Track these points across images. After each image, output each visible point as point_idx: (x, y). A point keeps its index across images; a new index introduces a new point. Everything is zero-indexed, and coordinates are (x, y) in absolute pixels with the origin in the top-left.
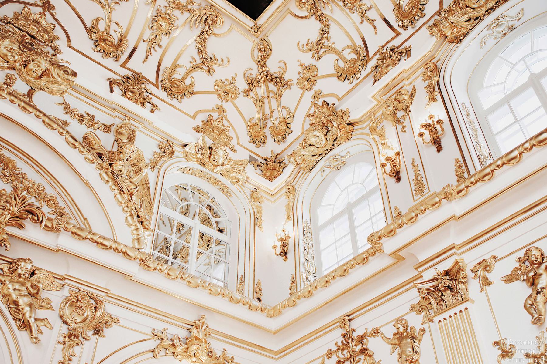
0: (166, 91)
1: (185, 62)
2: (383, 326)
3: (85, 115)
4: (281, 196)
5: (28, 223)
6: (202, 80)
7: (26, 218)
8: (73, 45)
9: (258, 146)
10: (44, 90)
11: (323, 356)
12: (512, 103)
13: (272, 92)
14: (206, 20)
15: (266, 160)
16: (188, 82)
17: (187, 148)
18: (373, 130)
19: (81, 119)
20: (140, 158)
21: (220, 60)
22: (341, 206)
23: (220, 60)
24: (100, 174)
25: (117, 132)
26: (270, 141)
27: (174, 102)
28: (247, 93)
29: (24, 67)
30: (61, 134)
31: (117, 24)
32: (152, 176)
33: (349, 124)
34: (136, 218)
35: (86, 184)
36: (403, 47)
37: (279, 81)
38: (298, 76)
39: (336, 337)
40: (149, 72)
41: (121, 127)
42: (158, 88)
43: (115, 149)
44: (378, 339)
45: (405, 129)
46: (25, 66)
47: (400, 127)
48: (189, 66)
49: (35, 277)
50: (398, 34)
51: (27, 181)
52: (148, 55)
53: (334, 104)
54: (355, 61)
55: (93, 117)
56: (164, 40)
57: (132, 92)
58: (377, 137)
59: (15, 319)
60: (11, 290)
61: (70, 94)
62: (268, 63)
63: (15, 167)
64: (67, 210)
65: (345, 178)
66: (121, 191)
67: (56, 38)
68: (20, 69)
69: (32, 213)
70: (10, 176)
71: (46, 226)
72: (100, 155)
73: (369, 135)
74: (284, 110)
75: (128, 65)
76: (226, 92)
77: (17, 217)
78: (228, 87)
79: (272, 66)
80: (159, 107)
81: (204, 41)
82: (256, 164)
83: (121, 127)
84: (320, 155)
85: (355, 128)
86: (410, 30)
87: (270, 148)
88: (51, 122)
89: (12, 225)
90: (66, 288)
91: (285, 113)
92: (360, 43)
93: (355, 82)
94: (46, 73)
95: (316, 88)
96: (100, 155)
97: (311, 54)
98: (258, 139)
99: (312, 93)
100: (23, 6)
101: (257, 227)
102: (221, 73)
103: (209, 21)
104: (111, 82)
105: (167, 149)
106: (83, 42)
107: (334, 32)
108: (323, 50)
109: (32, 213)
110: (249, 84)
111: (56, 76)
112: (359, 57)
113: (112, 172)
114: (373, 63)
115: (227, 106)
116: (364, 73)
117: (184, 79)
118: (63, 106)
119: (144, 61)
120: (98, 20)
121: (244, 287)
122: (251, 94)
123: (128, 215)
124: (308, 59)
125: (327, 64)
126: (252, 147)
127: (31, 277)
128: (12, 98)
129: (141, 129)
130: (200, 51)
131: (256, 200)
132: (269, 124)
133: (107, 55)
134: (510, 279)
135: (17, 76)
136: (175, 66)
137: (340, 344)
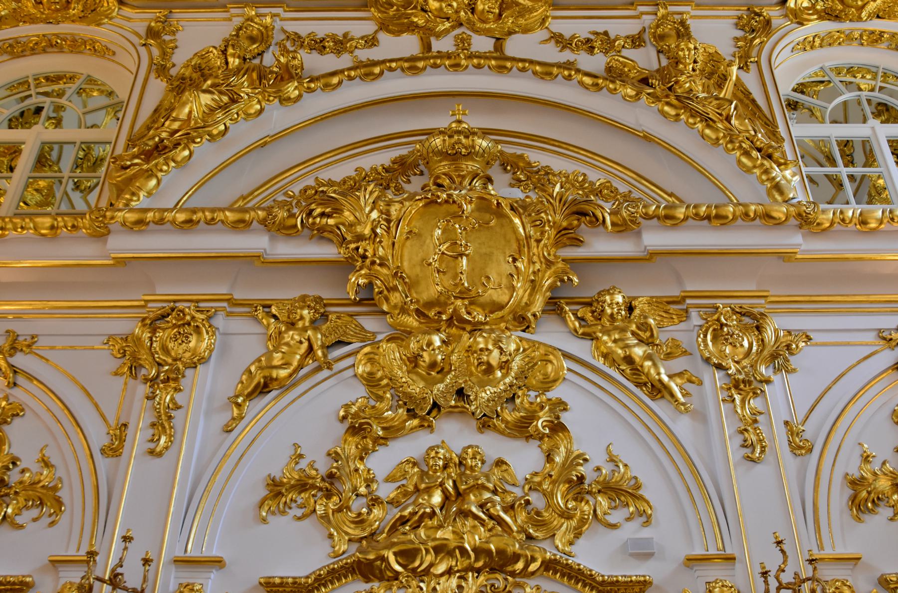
3: (592, 37)
5: (584, 230)
7: (579, 226)
10: (515, 32)
19: (589, 46)
20: (714, 59)
25: (654, 37)
29: (472, 13)
30: (569, 78)
32: (750, 81)
34: (755, 153)
35: (645, 137)
41: (658, 26)
43: (664, 62)
46: (473, 11)
49: (637, 312)
51: (554, 175)
55: (606, 33)
59: (639, 385)
60: (610, 344)
61: (554, 18)
64: (636, 195)
66: (708, 121)
68: (469, 19)
69: (584, 214)
70: (528, 178)
71: (613, 224)
77: (565, 229)
83: (658, 26)
88: (547, 71)
89: (565, 246)
90: (694, 313)
109: (584, 214)
113: (678, 98)
118: (553, 41)
123: (738, 154)
127: (630, 314)
128: (475, 61)
129: (694, 13)
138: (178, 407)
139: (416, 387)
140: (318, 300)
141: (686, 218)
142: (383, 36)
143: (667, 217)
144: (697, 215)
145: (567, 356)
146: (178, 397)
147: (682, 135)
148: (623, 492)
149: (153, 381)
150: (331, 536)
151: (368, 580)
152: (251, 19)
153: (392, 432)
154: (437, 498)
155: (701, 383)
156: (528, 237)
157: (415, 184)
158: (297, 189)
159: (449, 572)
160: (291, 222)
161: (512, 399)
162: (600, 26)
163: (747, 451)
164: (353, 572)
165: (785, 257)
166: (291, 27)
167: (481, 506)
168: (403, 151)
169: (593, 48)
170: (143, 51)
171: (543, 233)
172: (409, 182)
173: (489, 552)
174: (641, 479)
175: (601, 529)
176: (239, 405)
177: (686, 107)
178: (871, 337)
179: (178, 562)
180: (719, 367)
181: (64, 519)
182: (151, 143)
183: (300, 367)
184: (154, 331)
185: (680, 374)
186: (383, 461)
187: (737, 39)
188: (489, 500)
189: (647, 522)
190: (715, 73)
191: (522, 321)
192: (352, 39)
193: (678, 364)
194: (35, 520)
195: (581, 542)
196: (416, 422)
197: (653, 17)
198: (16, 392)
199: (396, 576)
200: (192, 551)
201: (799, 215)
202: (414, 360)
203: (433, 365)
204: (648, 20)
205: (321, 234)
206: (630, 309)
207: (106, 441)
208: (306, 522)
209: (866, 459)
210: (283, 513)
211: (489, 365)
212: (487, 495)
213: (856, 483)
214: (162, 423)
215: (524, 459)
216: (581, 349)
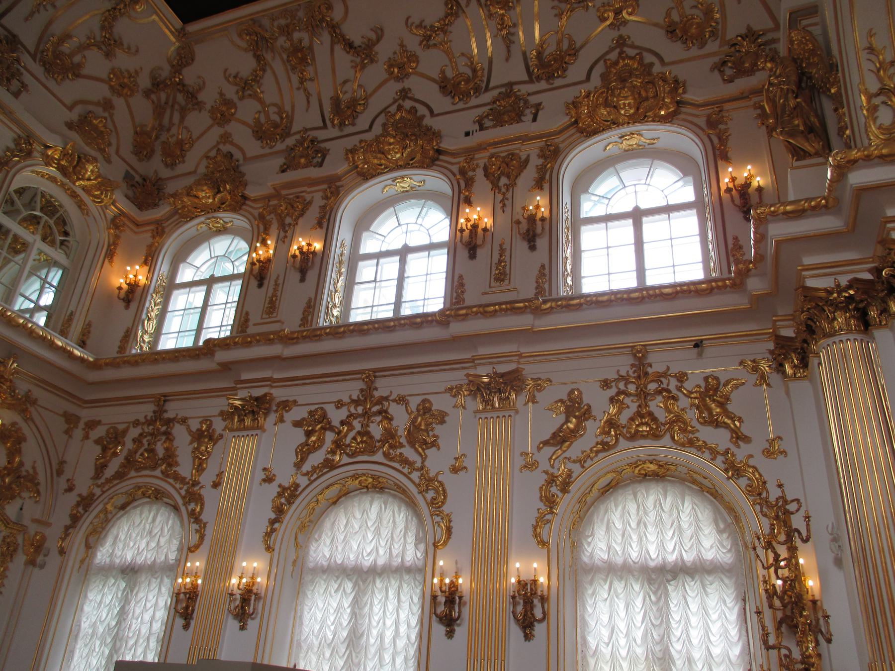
0: (44, 65)
4: (146, 231)
6: (96, 63)
11: (129, 423)
12: (382, 261)
15: (144, 180)
16: (77, 59)
18: (262, 217)
22: (204, 274)
23: (126, 46)
26: (158, 157)
27: (51, 84)
28: (147, 94)
33: (242, 196)
37: (192, 97)
39: (147, 410)
40: (28, 36)
42: (35, 60)
47: (282, 234)
50: (325, 126)
54: (276, 126)
58: (262, 227)
62: (185, 71)
65: (221, 245)
74: (184, 130)
76: (122, 84)
78: (126, 80)
79: (189, 76)
84: (202, 211)
85: (247, 202)
86: (335, 132)
87: (156, 166)
91: (183, 135)
93: (267, 150)
97: (235, 88)
101: (107, 260)
102: (123, 61)
107: (268, 79)
108: (250, 92)
110: (153, 85)
114: (291, 141)
115: (119, 102)
116: (280, 146)
117: (71, 55)
121: (70, 325)
122: (153, 97)
124: (231, 92)
126: (133, 160)
130: (103, 28)
131: (117, 227)
132: (163, 138)
134: (297, 424)
136: (67, 37)
137: (149, 418)
187: (8, 149)
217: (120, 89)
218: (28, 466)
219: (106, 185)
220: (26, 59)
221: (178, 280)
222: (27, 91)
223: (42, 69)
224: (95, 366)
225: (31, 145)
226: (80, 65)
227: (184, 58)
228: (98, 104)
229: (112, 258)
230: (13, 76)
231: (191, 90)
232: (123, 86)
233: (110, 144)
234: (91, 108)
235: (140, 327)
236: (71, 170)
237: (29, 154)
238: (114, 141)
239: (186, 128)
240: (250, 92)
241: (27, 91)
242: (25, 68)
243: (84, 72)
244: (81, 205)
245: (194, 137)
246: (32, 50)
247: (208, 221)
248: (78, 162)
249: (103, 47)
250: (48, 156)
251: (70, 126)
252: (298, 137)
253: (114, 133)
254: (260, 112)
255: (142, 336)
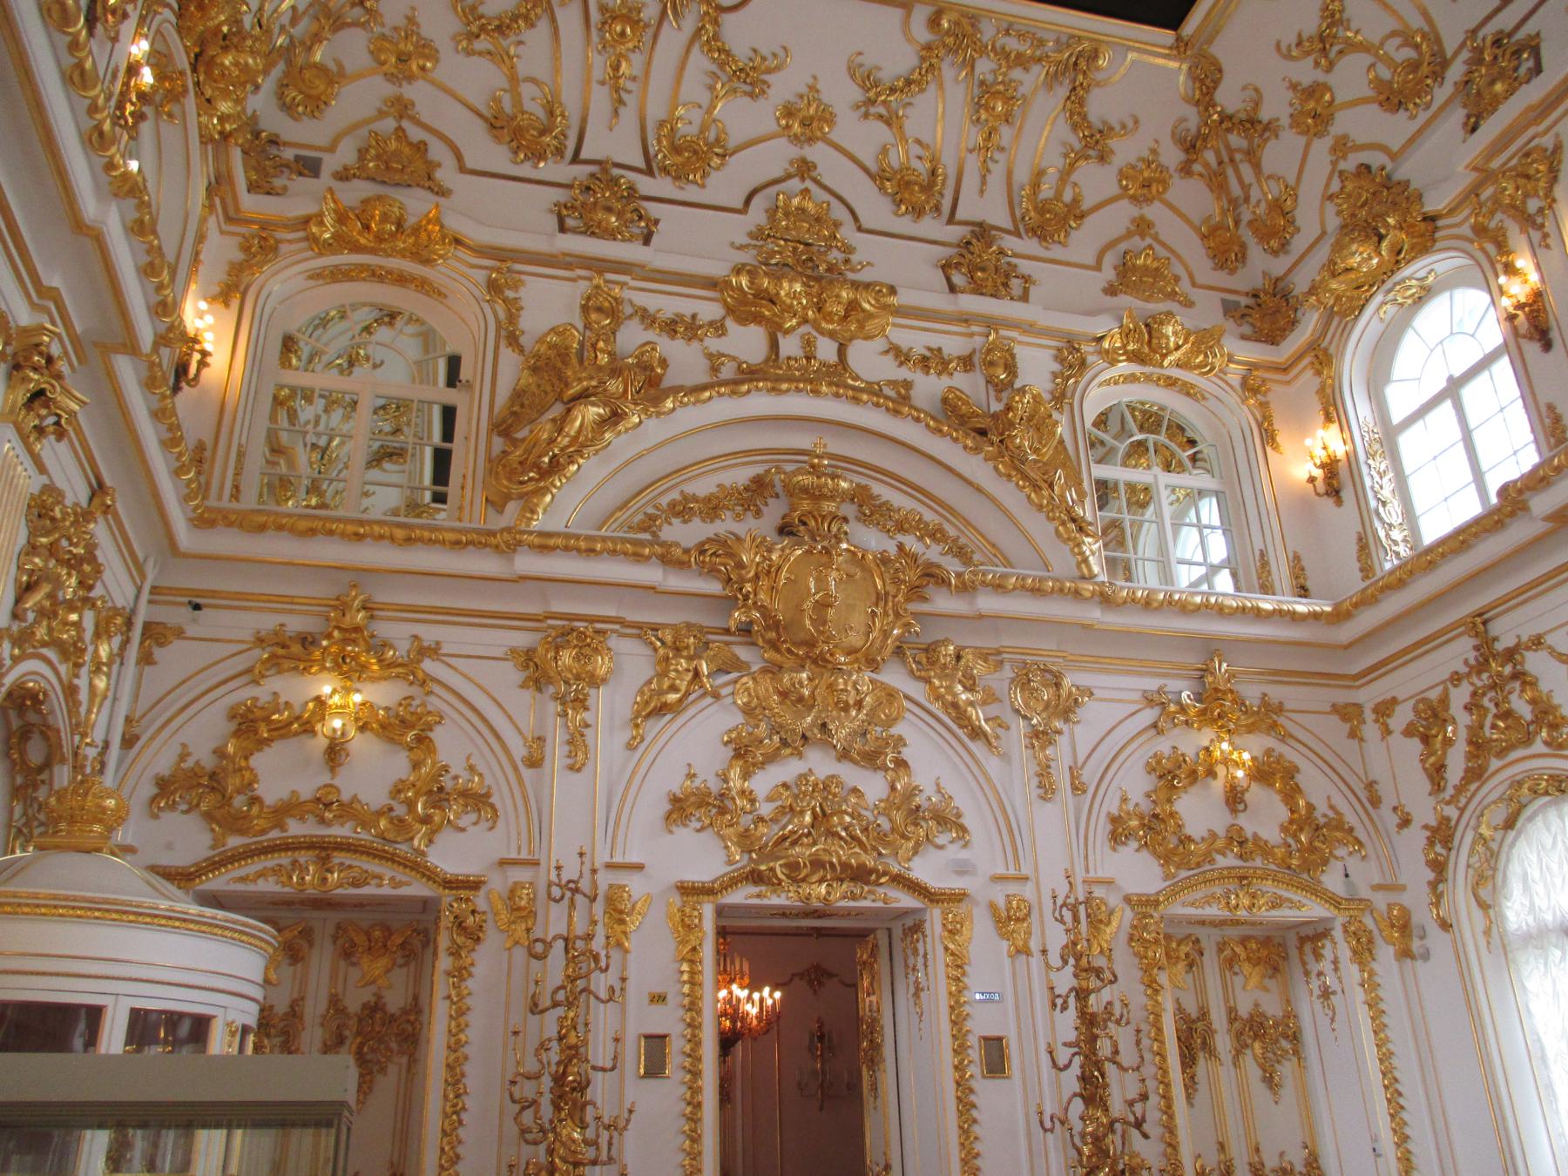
1: (1054, 165)
2: (1550, 631)
3: (928, 354)
5: (931, 590)
6: (1095, 181)
8: (866, 224)
9: (1232, 271)
11: (1443, 682)
13: (1239, 150)
14: (1076, 64)
15: (1255, 296)
16: (1068, 196)
17: (1106, 344)
18: (1480, 231)
19: (924, 363)
21: (1117, 127)
23: (1117, 127)
24: (996, 468)
26: (1255, 252)
27: (1057, 252)
28: (1186, 170)
31: (918, 142)
36: (1520, 35)
37: (1253, 125)
38: (1291, 110)
39: (1463, 650)
40: (998, 215)
42: (1020, 236)
44: (1542, 654)
45: (1549, 241)
47: (1536, 236)
48: (1060, 163)
49: (963, 662)
52: (984, 177)
53: (1383, 169)
54: (1414, 66)
55: (940, 350)
56: (1006, 134)
57: (983, 270)
58: (1491, 248)
59: (961, 727)
61: (894, 325)
63: (872, 497)
64: (963, 541)
65: (1433, 317)
66: (1036, 488)
67: (837, 225)
72: (983, 433)
73: (1472, 241)
74: (1272, 183)
75: (961, 214)
76: (1145, 184)
78: (1146, 175)
79: (1229, 97)
80: (1035, 277)
81: (1081, 105)
82: (1237, 315)
83: (989, 351)
84: (1371, 286)
85: (1440, 223)
87: (1260, 265)
90: (1007, 666)
91: (1273, 190)
92: (1416, 22)
93: (1423, 116)
94: (853, 306)
95: (1336, 129)
96: (983, 433)
97: (1310, 61)
98: (1226, 254)
99: (1327, 142)
100: (773, 190)
101: (1268, 449)
102: (1126, 151)
103: (1083, 64)
104: (943, 267)
105: (1072, 359)
106: (874, 207)
108: (1336, 48)
110: (1187, 151)
111: (867, 306)
112: (1420, 54)
114: (1456, 72)
116: (1442, 93)
117: (1058, 195)
119: (982, 192)
120: (884, 151)
122: (1197, 168)
124: (1305, 71)
125: (1351, 78)
126: (1221, 279)
129: (1021, 338)
131: (1255, 391)
132: (1246, 216)
133: (918, 212)
135: (815, 333)
137: (1472, 662)
138: (587, 726)
139: (788, 719)
140: (701, 629)
141: (1015, 589)
142: (730, 324)
143: (999, 586)
144: (1023, 587)
145: (907, 697)
146: (586, 715)
147: (1010, 494)
148: (947, 819)
149: (561, 699)
150: (727, 847)
151: (756, 883)
152: (597, 287)
153: (771, 758)
154: (808, 818)
155: (1008, 728)
156: (887, 594)
157: (774, 511)
158: (665, 501)
159: (820, 881)
160: (685, 558)
161: (864, 734)
162: (935, 341)
163: (1041, 791)
164: (747, 878)
165: (1086, 627)
166: (641, 299)
167: (846, 829)
168: (759, 470)
169: (928, 367)
170: (486, 306)
171: (899, 590)
172: (766, 504)
173: (851, 866)
174: (962, 809)
175: (932, 849)
176: (637, 726)
177: (1016, 468)
178: (1137, 696)
179: (610, 866)
180: (1025, 717)
181: (501, 824)
182: (546, 460)
183: (687, 694)
184: (557, 649)
185: (992, 719)
186: (764, 782)
187: (1055, 375)
188: (850, 824)
189: (966, 845)
190: (1040, 424)
191: (873, 664)
192: (700, 327)
193: (993, 710)
194: (475, 824)
195: (916, 859)
196: (788, 751)
197: (983, 339)
198: (432, 699)
199: (780, 882)
200: (618, 859)
201: (1102, 594)
202: (784, 695)
203: (801, 699)
204: (979, 340)
205: (713, 572)
206: (958, 658)
207: (523, 752)
208: (703, 835)
209: (1124, 800)
210: (685, 826)
211: (846, 703)
212: (848, 819)
213: (1115, 820)
214: (577, 741)
215: (874, 787)
216: (916, 690)
217: (1145, 191)
218: (1322, 808)
219: (1204, 340)
220: (1010, 243)
221: (1397, 417)
222: (1034, 283)
223: (1035, 240)
224: (1339, 616)
225: (1078, 350)
226: (1076, 201)
227: (1207, 78)
228: (1129, 234)
229: (1273, 439)
230: (1007, 276)
231: (1243, 116)
232: (1146, 185)
233: (1177, 279)
234: (1123, 246)
235: (1377, 524)
236: (1146, 350)
237: (1083, 364)
238: (1179, 270)
239: (1270, 177)
240: (1336, 48)
241: (1034, 283)
242: (1015, 255)
243: (1086, 205)
244: (1188, 390)
245: (1292, 182)
246: (1010, 226)
247: (1391, 296)
248: (1150, 333)
249: (1091, 152)
250: (1107, 352)
251: (1111, 291)
252: (1465, 55)
253: (1173, 259)
254: (1372, 66)
255: (1388, 536)
